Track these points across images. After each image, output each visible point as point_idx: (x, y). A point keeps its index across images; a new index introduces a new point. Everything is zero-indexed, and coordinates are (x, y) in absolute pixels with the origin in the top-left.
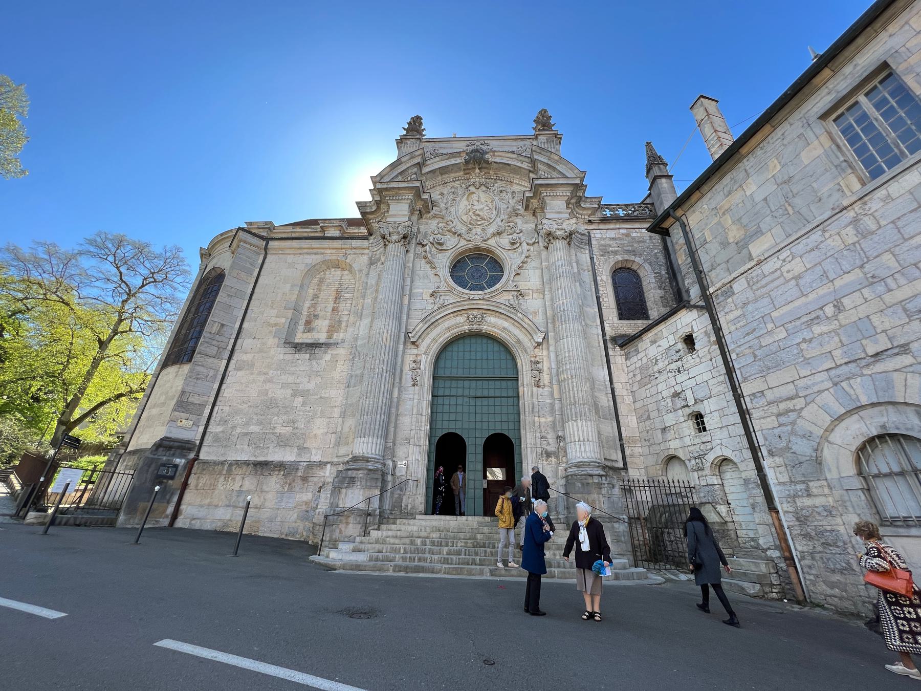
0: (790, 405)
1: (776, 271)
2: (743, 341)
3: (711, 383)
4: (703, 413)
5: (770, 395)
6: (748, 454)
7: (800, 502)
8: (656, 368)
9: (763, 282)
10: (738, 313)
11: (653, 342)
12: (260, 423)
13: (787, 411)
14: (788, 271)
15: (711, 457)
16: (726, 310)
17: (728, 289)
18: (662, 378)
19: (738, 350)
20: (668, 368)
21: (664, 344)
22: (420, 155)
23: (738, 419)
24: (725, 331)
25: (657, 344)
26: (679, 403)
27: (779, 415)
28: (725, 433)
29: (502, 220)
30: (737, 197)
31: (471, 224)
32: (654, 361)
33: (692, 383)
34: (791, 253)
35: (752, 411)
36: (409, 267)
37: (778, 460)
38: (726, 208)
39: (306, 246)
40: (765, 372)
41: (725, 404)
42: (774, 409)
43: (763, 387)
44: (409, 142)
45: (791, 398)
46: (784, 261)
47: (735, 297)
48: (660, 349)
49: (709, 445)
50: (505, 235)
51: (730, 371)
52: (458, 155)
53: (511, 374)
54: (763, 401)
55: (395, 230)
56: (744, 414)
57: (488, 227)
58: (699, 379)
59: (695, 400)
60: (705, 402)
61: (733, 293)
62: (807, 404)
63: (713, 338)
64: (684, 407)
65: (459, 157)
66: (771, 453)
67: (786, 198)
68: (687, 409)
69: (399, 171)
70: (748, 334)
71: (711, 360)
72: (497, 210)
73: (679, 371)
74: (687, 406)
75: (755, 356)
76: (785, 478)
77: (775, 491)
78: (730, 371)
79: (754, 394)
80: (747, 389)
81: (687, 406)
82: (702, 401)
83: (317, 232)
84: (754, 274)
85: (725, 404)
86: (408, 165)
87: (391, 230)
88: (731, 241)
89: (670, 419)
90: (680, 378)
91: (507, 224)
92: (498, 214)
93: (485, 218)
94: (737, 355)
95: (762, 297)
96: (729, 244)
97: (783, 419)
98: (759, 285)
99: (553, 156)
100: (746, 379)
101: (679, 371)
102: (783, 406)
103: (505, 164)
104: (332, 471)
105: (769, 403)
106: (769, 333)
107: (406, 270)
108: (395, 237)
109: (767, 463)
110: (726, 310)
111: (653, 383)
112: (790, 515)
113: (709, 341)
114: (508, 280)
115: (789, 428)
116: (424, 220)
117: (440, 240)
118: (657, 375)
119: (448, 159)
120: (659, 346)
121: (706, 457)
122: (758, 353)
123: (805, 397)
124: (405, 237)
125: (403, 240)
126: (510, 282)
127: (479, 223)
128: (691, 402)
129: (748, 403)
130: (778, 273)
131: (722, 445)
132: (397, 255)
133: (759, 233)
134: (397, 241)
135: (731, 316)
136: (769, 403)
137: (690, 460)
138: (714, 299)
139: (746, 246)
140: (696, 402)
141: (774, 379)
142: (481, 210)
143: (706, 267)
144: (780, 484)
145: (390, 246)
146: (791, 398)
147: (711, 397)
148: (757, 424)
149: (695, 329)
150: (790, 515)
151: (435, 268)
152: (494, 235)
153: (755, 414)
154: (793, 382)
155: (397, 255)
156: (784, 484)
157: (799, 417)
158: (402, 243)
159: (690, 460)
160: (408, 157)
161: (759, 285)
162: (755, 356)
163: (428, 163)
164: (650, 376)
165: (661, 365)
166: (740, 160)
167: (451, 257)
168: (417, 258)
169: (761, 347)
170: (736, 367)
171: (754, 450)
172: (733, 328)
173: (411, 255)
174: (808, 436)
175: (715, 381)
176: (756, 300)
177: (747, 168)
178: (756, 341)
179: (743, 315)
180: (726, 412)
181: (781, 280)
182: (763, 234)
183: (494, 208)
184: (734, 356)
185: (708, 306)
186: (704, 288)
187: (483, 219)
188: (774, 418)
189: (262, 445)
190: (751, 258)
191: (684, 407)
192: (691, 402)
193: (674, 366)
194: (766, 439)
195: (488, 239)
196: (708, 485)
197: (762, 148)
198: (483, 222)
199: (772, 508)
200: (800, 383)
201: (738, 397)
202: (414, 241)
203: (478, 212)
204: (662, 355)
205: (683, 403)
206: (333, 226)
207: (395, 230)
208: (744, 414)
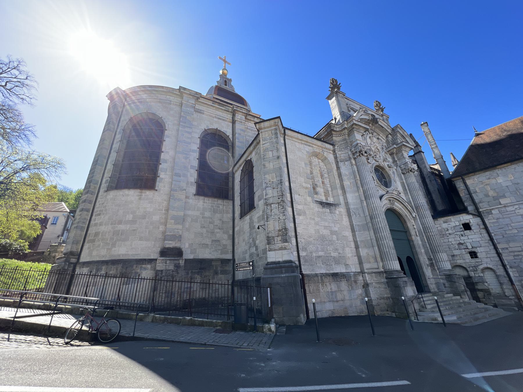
1: (512, 211)
2: (497, 230)
5: (510, 249)
6: (501, 267)
9: (507, 213)
10: (495, 221)
11: (444, 222)
12: (323, 250)
13: (518, 255)
14: (518, 212)
15: (481, 267)
16: (489, 218)
19: (495, 233)
20: (455, 233)
21: (453, 224)
25: (448, 223)
27: (514, 256)
28: (489, 260)
30: (493, 181)
32: (446, 230)
34: (519, 207)
37: (514, 270)
38: (488, 183)
39: (305, 140)
40: (508, 242)
41: (489, 250)
42: (512, 254)
43: (507, 246)
46: (516, 208)
48: (449, 226)
49: (480, 263)
51: (492, 239)
54: (506, 251)
56: (499, 255)
63: (482, 226)
66: (511, 267)
67: (517, 189)
68: (467, 250)
70: (500, 229)
71: (481, 234)
74: (468, 248)
75: (503, 236)
78: (492, 239)
80: (499, 246)
81: (468, 248)
83: (229, 111)
84: (502, 210)
85: (489, 250)
90: (462, 238)
94: (495, 234)
95: (506, 218)
96: (489, 196)
97: (516, 257)
98: (505, 214)
99: (405, 132)
102: (516, 253)
103: (381, 126)
104: (369, 277)
109: (510, 271)
110: (489, 218)
112: (520, 286)
115: (519, 260)
119: (365, 115)
120: (449, 224)
121: (479, 267)
122: (505, 235)
128: (470, 247)
130: (513, 212)
131: (487, 263)
133: (504, 196)
137: (469, 268)
138: (482, 213)
140: (473, 247)
141: (511, 245)
144: (515, 276)
147: (481, 247)
148: (505, 257)
149: (471, 222)
150: (520, 286)
154: (520, 247)
156: (517, 277)
159: (469, 268)
161: (505, 214)
162: (503, 236)
164: (443, 235)
165: (450, 232)
166: (495, 169)
169: (506, 234)
170: (494, 238)
171: (504, 266)
172: (492, 225)
177: (498, 173)
178: (504, 232)
179: (497, 222)
181: (515, 214)
182: (506, 197)
184: (493, 235)
185: (479, 214)
188: (513, 257)
189: (328, 264)
194: (508, 263)
196: (479, 276)
197: (505, 169)
201: (496, 248)
204: (451, 228)
206: (242, 112)
208: (499, 255)
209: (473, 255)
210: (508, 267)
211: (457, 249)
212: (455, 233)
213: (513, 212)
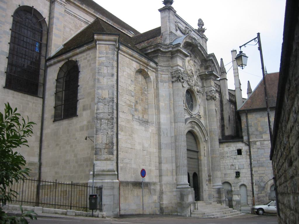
0: (262, 175)
3: (244, 165)
4: (240, 172)
5: (259, 172)
6: (250, 184)
7: (259, 195)
8: (226, 155)
17: (255, 142)
18: (228, 159)
19: (254, 159)
20: (231, 156)
21: (231, 149)
23: (250, 176)
24: (252, 153)
25: (229, 148)
26: (233, 167)
32: (226, 153)
33: (239, 163)
35: (254, 175)
37: (257, 186)
40: (259, 167)
42: (259, 175)
43: (258, 170)
45: (263, 174)
47: (256, 146)
48: (229, 150)
51: (251, 164)
53: (195, 149)
56: (252, 175)
58: (241, 163)
59: (239, 168)
60: (242, 170)
61: (256, 144)
62: (266, 176)
63: (249, 153)
64: (234, 169)
68: (235, 170)
73: (235, 159)
76: (258, 190)
77: (255, 193)
78: (251, 164)
79: (255, 171)
80: (254, 169)
81: (236, 169)
82: (241, 169)
88: (259, 130)
89: (228, 172)
90: (235, 161)
100: (254, 167)
101: (235, 159)
102: (261, 175)
105: (258, 174)
106: (262, 158)
109: (255, 187)
111: (225, 159)
113: (247, 154)
118: (226, 157)
120: (229, 149)
121: (239, 184)
123: (266, 174)
128: (237, 168)
129: (253, 172)
135: (254, 150)
136: (258, 174)
139: (262, 134)
143: (250, 133)
146: (263, 174)
147: (244, 169)
149: (243, 149)
153: (254, 175)
157: (264, 178)
165: (228, 155)
171: (252, 183)
174: (264, 182)
175: (246, 165)
176: (261, 149)
180: (247, 173)
182: (266, 134)
184: (252, 160)
185: (249, 144)
186: (249, 139)
190: (262, 138)
191: (234, 169)
192: (237, 168)
193: (234, 157)
199: (253, 196)
200: (266, 171)
201: (251, 170)
204: (230, 152)
205: (235, 168)
209: (238, 174)
210: (254, 184)
211: (229, 169)
212: (231, 156)
213: (267, 145)
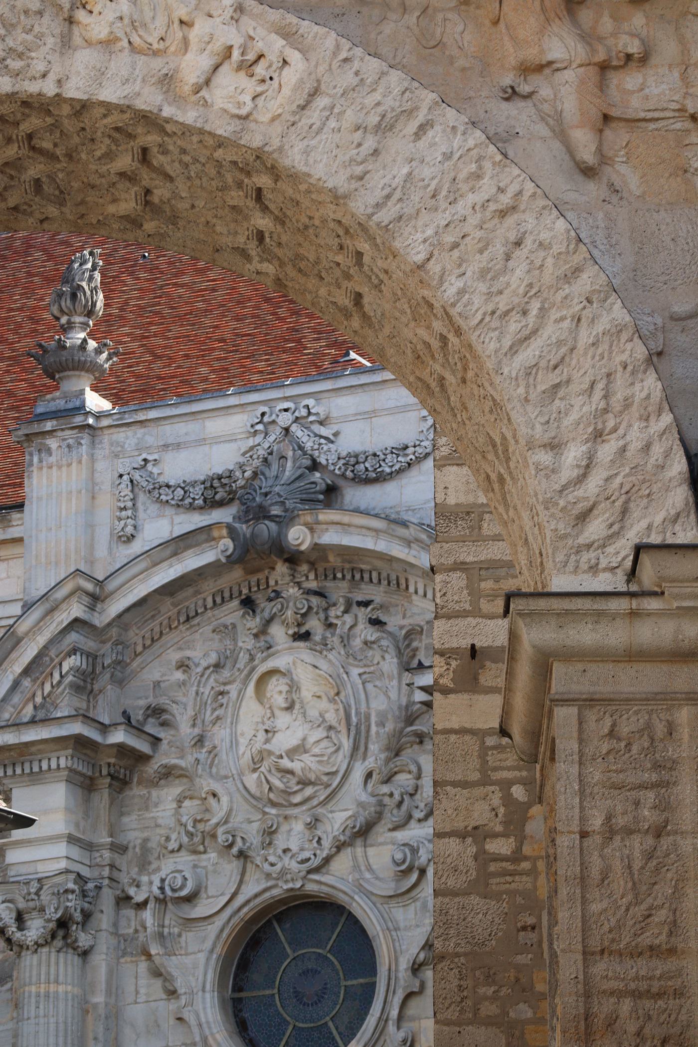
22: (72, 594)
29: (369, 775)
31: (274, 804)
36: (95, 1006)
44: (53, 443)
50: (381, 833)
52: (203, 537)
55: (31, 904)
57: (329, 806)
65: (207, 541)
69: (18, 669)
72: (353, 729)
86: (42, 640)
87: (22, 905)
91: (385, 789)
92: (355, 748)
93: (313, 777)
107: (90, 1018)
108: (35, 929)
114: (383, 1020)
116: (136, 791)
117: (182, 888)
124: (63, 924)
125: (61, 933)
126: (391, 1027)
127: (297, 799)
132: (47, 995)
134: (41, 941)
142: (292, 753)
145: (29, 960)
151: (172, 993)
152: (340, 847)
155: (47, 995)
158: (58, 943)
160: (35, 614)
163: (111, 586)
167: (218, 949)
168: (124, 954)
173: (100, 961)
183: (343, 728)
187: (304, 783)
195: (327, 860)
198: (309, 791)
202: (107, 898)
203: (286, 763)
207: (31, 904)
